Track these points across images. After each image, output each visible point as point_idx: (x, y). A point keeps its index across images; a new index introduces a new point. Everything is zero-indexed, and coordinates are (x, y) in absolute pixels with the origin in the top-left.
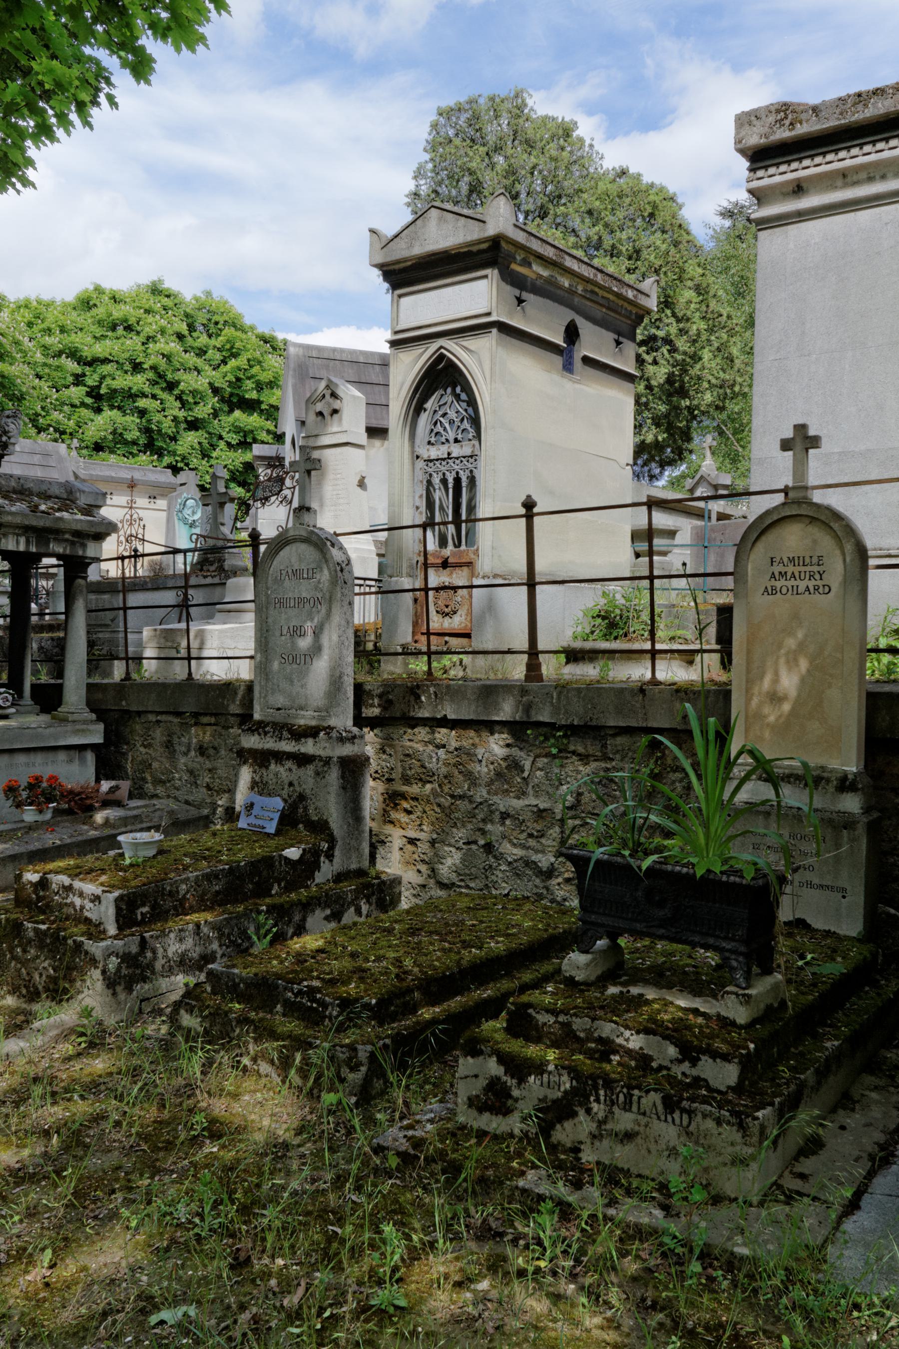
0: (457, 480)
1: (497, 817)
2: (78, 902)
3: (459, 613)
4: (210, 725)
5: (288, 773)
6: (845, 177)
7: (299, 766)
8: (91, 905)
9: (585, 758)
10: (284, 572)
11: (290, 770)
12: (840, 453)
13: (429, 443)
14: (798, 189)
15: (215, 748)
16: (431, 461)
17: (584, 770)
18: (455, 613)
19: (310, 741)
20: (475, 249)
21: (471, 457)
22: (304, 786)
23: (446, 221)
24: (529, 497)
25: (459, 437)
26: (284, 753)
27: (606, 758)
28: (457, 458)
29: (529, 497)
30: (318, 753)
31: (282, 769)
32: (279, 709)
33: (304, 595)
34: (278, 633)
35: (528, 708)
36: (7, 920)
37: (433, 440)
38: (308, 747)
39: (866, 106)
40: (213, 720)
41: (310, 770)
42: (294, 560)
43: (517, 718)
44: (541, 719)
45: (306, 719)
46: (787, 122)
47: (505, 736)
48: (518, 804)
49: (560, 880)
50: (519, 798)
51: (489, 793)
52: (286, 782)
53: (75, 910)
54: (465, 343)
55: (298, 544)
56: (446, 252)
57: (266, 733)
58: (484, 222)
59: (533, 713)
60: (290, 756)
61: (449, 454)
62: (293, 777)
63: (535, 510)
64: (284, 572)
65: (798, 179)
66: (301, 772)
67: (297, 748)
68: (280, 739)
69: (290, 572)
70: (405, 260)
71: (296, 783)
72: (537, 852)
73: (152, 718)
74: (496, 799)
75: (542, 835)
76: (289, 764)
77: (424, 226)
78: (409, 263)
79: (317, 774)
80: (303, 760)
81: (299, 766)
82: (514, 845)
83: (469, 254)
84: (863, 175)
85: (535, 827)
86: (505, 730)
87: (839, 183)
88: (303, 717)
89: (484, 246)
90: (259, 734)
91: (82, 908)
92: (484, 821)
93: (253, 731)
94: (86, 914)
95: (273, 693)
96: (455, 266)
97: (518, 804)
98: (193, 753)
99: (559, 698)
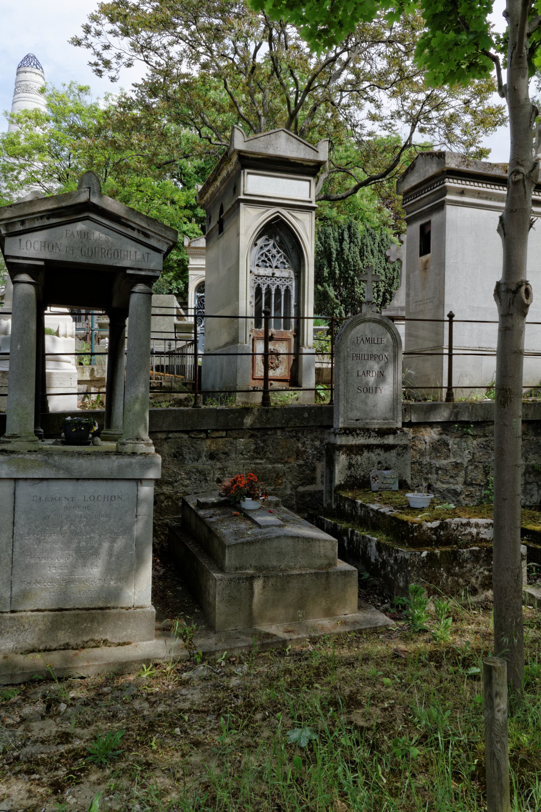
0: (278, 290)
1: (434, 470)
2: (474, 531)
3: (280, 367)
4: (222, 437)
5: (377, 456)
6: (479, 195)
7: (385, 451)
8: (486, 530)
9: (475, 437)
10: (360, 339)
11: (379, 454)
12: (478, 307)
13: (258, 265)
14: (462, 192)
15: (225, 453)
16: (259, 276)
17: (475, 442)
18: (277, 367)
19: (391, 437)
20: (305, 163)
21: (288, 278)
22: (389, 463)
23: (291, 142)
24: (451, 312)
25: (279, 265)
26: (374, 445)
27: (485, 436)
28: (278, 278)
29: (451, 312)
30: (397, 443)
31: (372, 455)
32: (357, 420)
33: (375, 353)
34: (355, 374)
35: (457, 414)
36: (442, 553)
37: (260, 264)
38: (390, 440)
39: (493, 169)
40: (224, 434)
41: (393, 453)
42: (367, 332)
43: (451, 420)
44: (463, 419)
45: (376, 425)
46: (466, 164)
47: (439, 429)
48: (444, 462)
49: (464, 496)
50: (445, 459)
51: (430, 459)
52: (376, 462)
53: (473, 536)
54: (291, 212)
55: (371, 323)
56: (287, 159)
57: (358, 435)
58: (317, 152)
59: (459, 416)
60: (378, 446)
61: (273, 274)
62: (381, 458)
63: (454, 319)
64: (360, 339)
65: (464, 189)
66: (387, 455)
67: (381, 442)
68: (369, 437)
69: (364, 339)
70: (258, 154)
71: (383, 462)
72: (454, 484)
73: (163, 436)
74: (433, 461)
75: (457, 475)
76: (378, 451)
77: (276, 139)
78: (260, 157)
79: (399, 454)
80: (388, 448)
81: (385, 451)
82: (443, 483)
83: (301, 165)
84: (485, 196)
85: (453, 472)
86: (439, 426)
87: (476, 195)
88: (373, 424)
89: (312, 164)
90: (353, 435)
91: (478, 534)
92: (427, 473)
93: (347, 434)
94: (481, 536)
95: (351, 411)
96: (290, 169)
97: (444, 462)
98: (204, 459)
99: (472, 409)
